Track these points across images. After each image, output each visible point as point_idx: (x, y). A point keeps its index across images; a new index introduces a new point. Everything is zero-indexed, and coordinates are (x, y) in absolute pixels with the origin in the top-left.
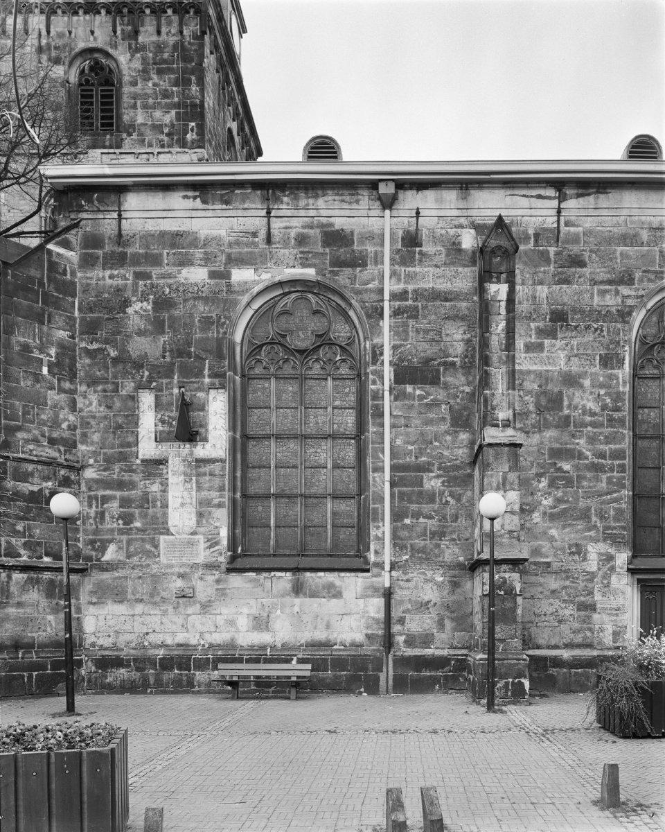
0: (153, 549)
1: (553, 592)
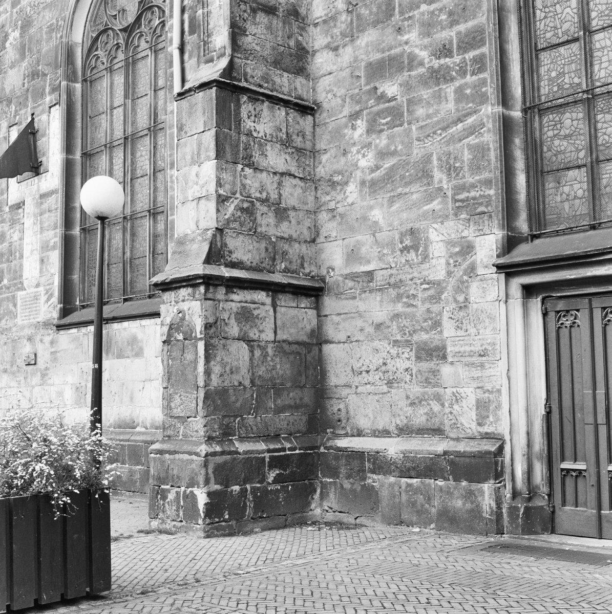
1: (378, 326)
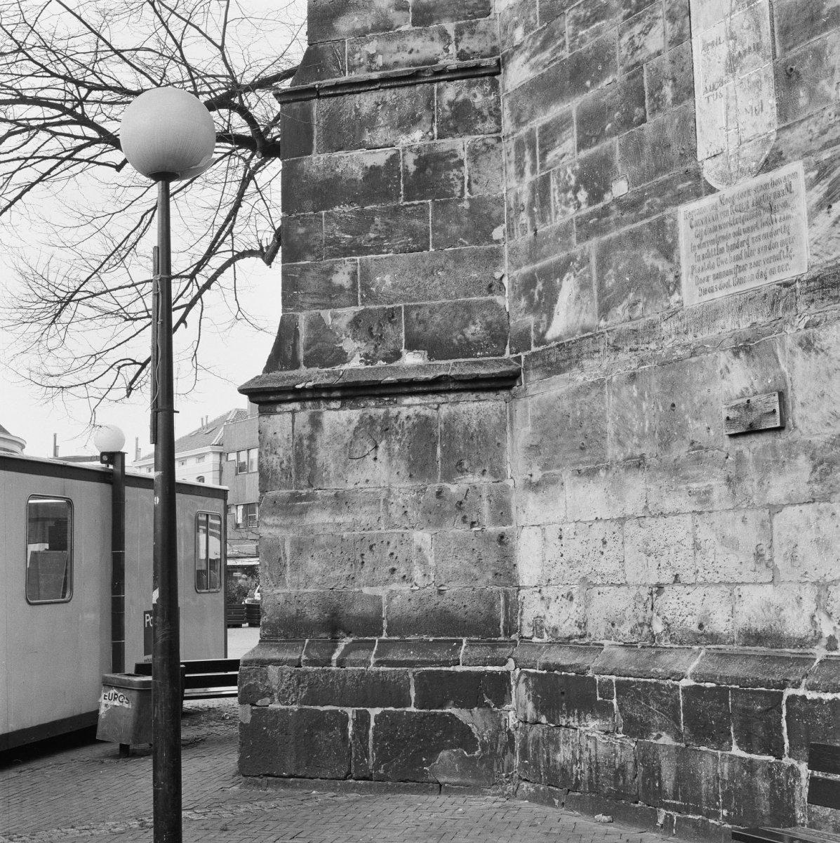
0: (661, 264)
